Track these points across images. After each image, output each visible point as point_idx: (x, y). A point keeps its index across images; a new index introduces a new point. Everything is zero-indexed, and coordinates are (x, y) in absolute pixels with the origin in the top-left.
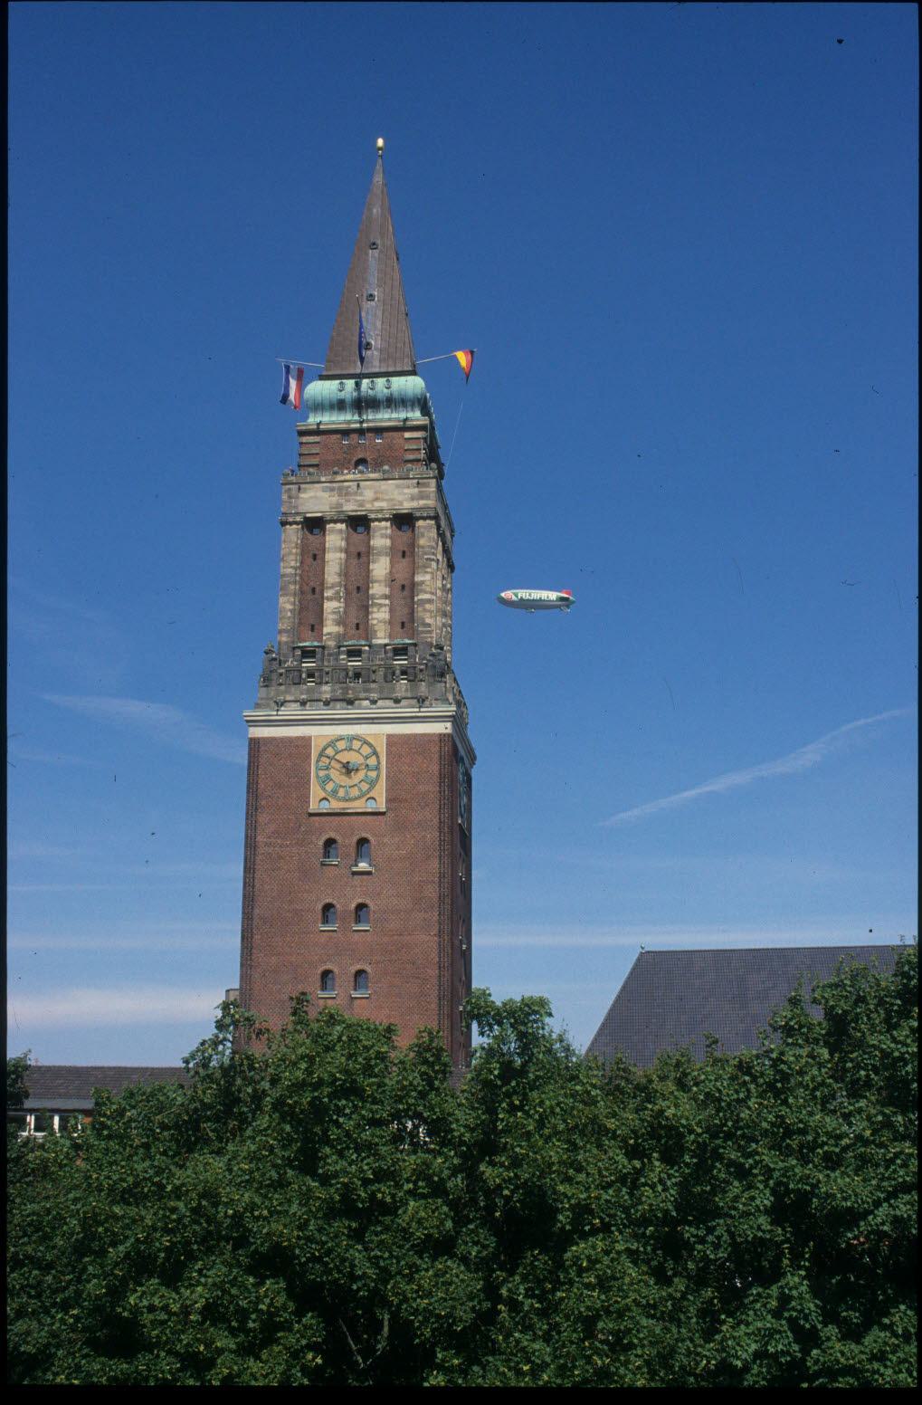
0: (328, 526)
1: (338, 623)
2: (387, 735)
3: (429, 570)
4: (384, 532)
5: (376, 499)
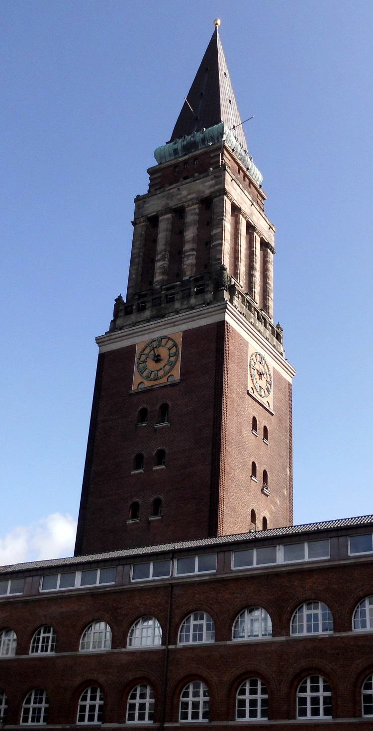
0: (160, 218)
1: (163, 273)
2: (184, 332)
3: (219, 226)
4: (193, 212)
5: (189, 194)
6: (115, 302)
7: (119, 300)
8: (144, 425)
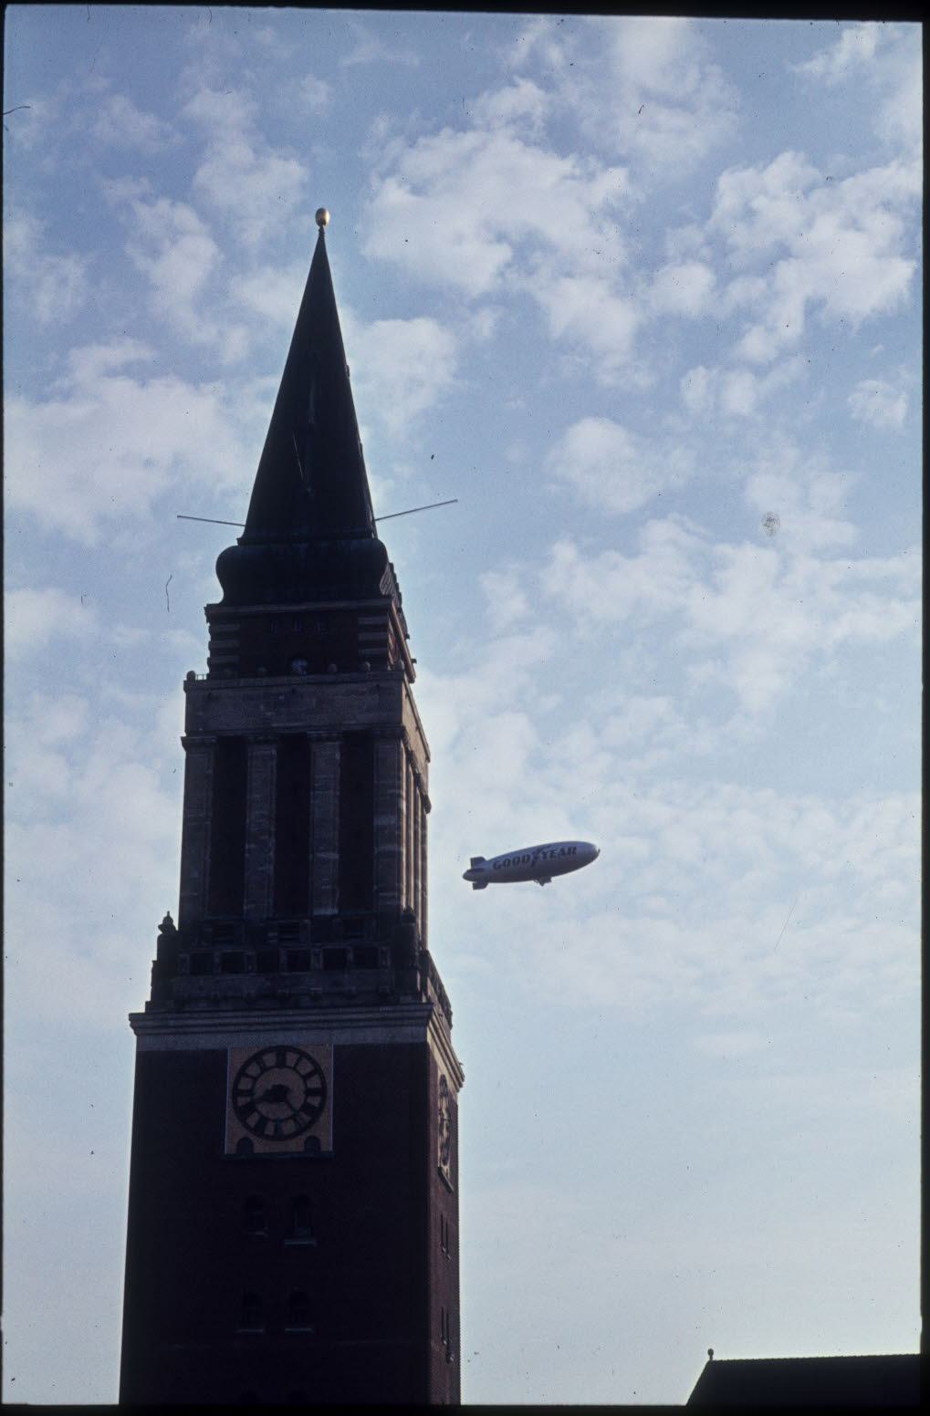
6: (160, 933)
7: (167, 924)
8: (257, 1233)
